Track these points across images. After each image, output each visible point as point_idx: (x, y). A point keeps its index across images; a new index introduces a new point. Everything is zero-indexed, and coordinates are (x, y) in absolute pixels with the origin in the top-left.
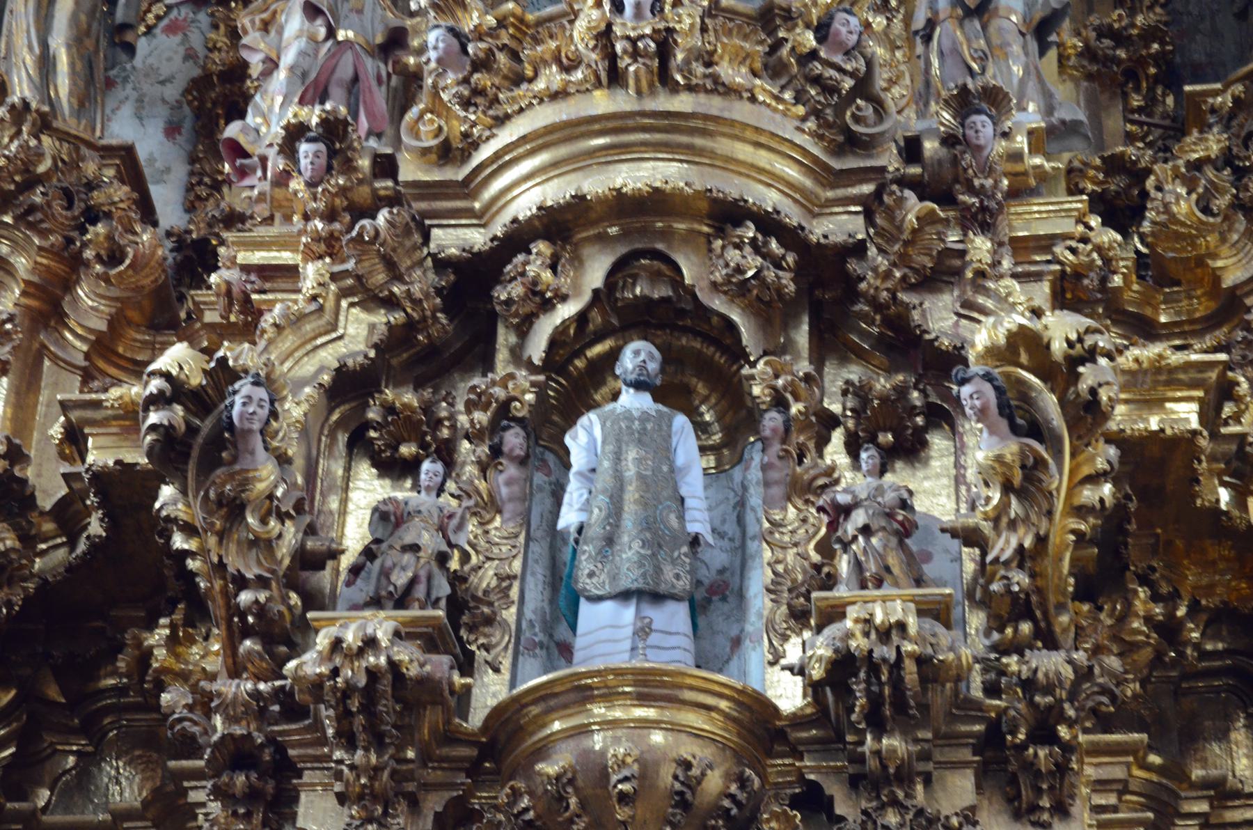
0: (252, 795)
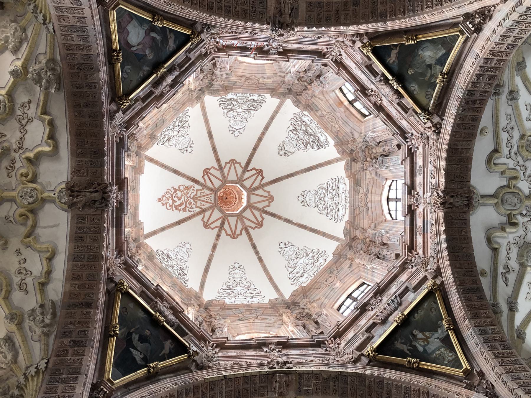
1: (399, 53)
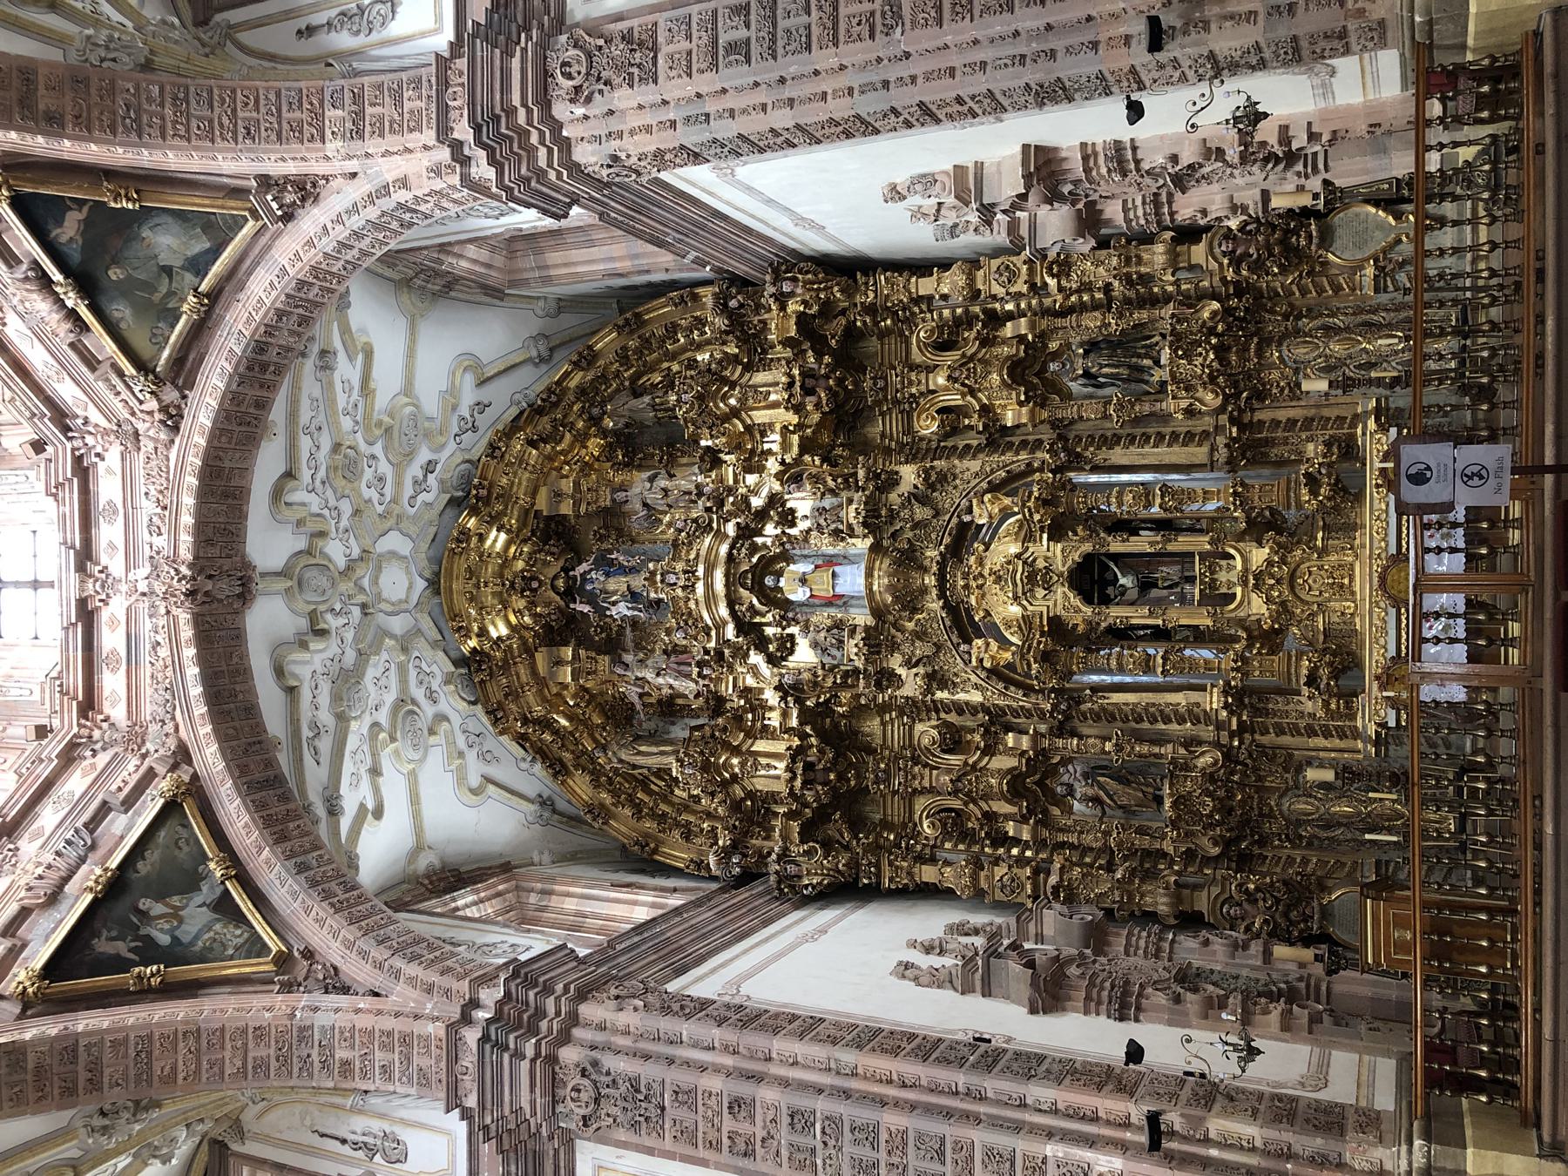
1: (87, 224)
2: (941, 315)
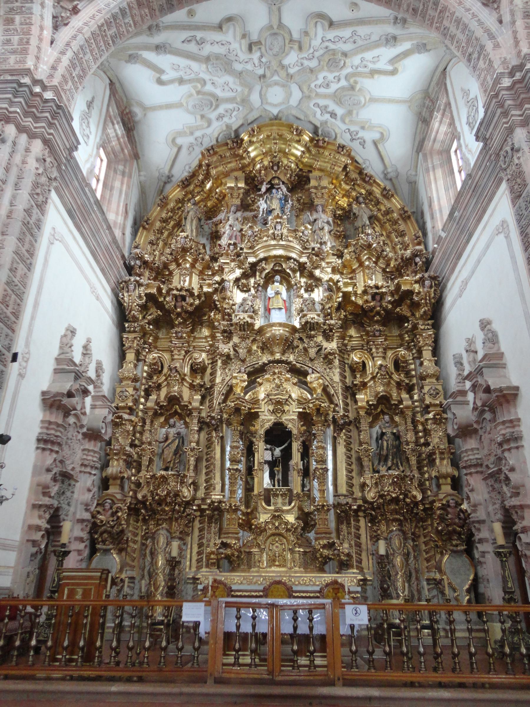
0: (227, 337)
2: (411, 364)
